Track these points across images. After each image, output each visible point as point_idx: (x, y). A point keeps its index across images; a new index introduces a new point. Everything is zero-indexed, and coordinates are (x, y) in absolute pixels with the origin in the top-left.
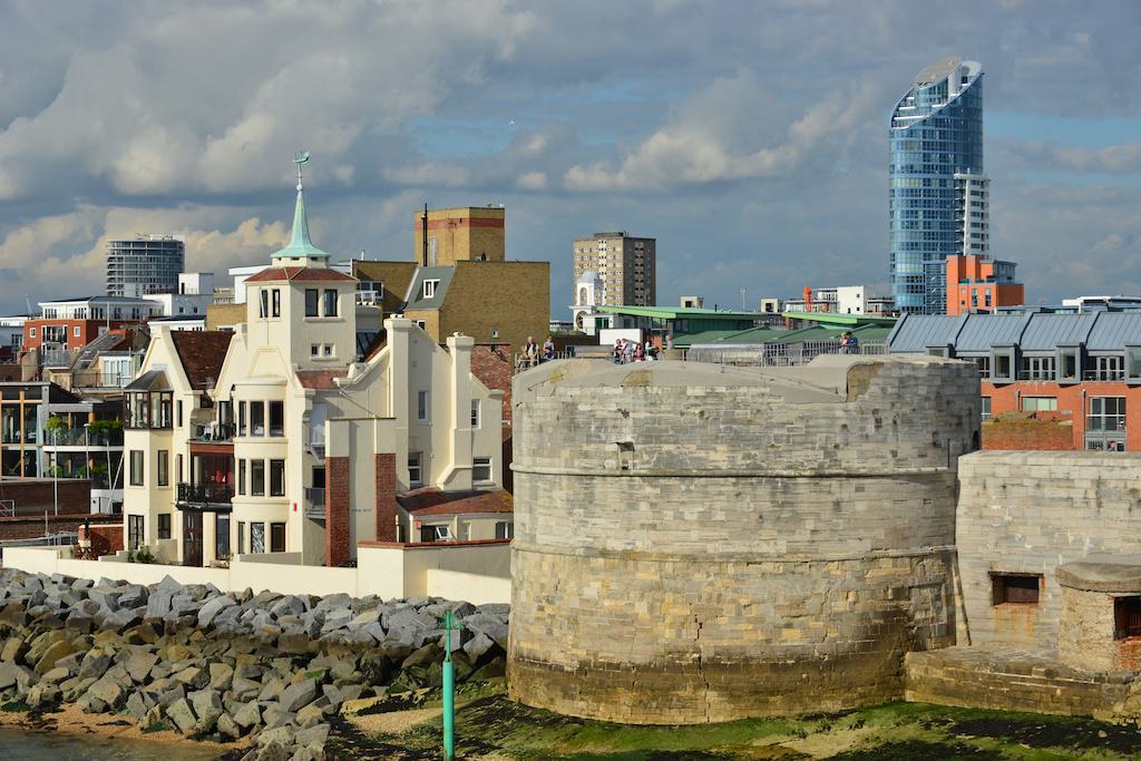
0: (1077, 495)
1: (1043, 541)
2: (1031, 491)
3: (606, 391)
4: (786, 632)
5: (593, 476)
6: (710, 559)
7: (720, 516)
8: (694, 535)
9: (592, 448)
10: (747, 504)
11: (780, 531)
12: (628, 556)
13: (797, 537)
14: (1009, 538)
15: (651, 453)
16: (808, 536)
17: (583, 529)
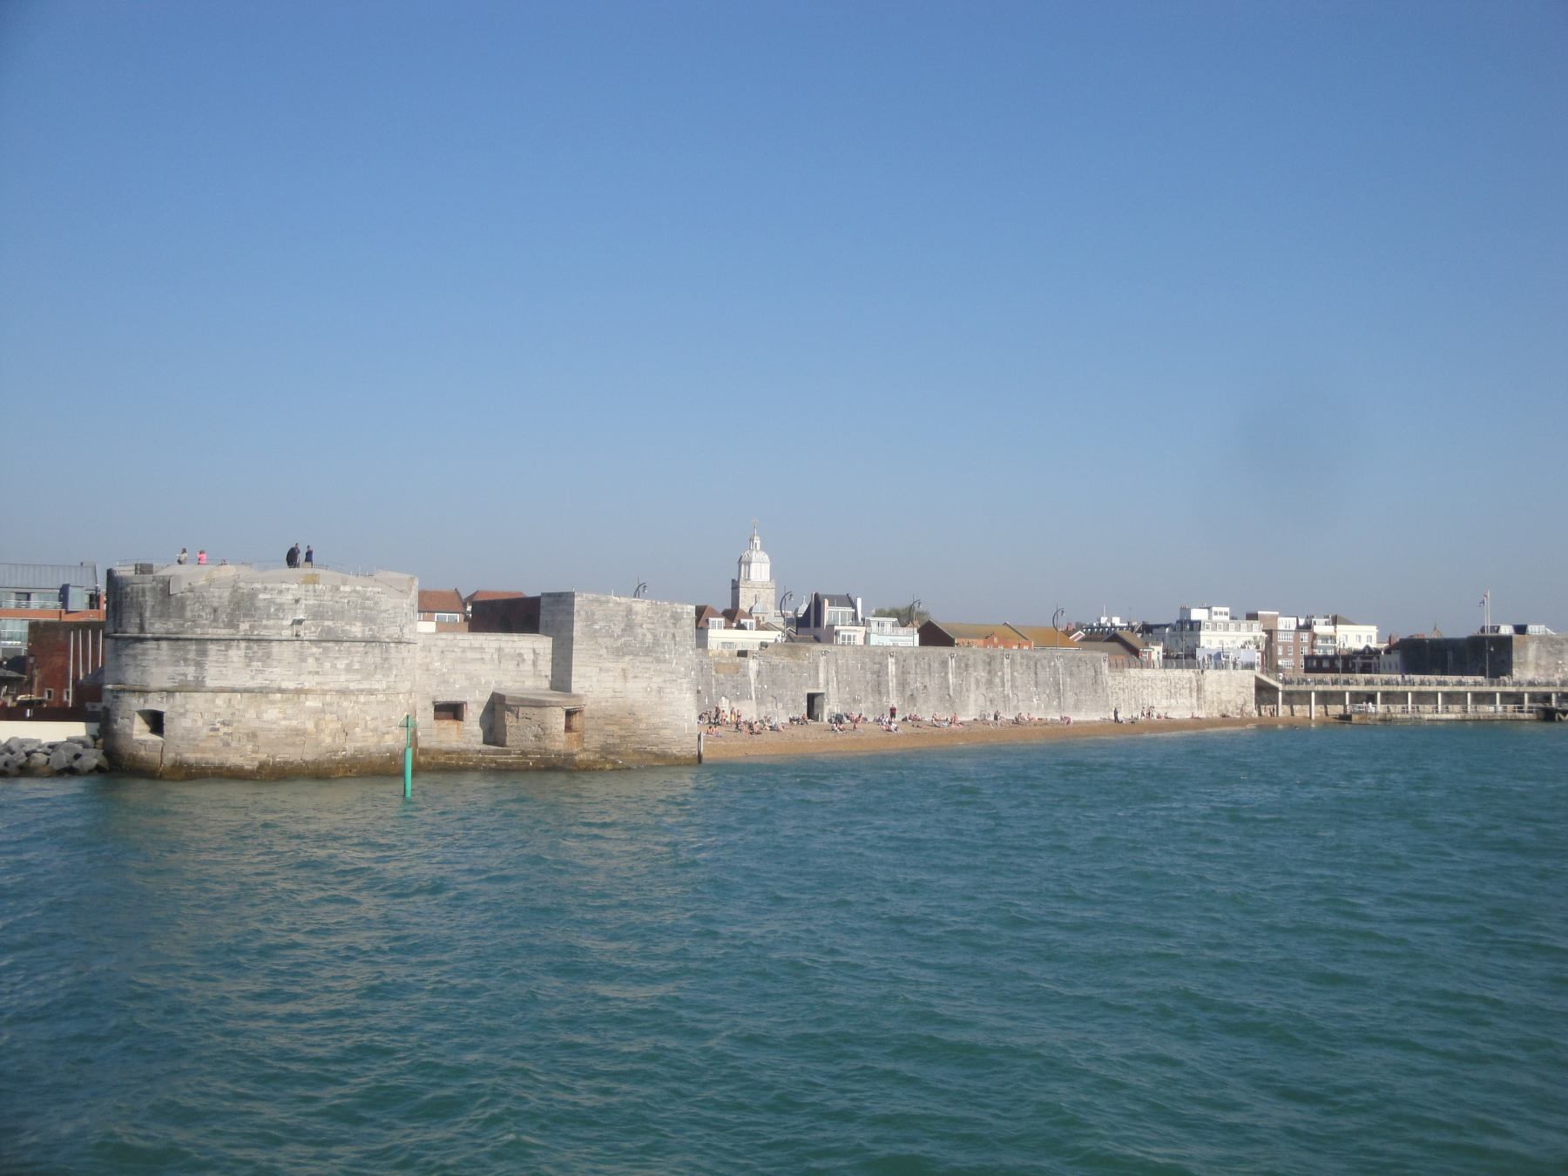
1: (466, 683)
6: (352, 692)
7: (357, 666)
8: (343, 678)
9: (271, 622)
10: (370, 659)
12: (299, 692)
14: (445, 682)
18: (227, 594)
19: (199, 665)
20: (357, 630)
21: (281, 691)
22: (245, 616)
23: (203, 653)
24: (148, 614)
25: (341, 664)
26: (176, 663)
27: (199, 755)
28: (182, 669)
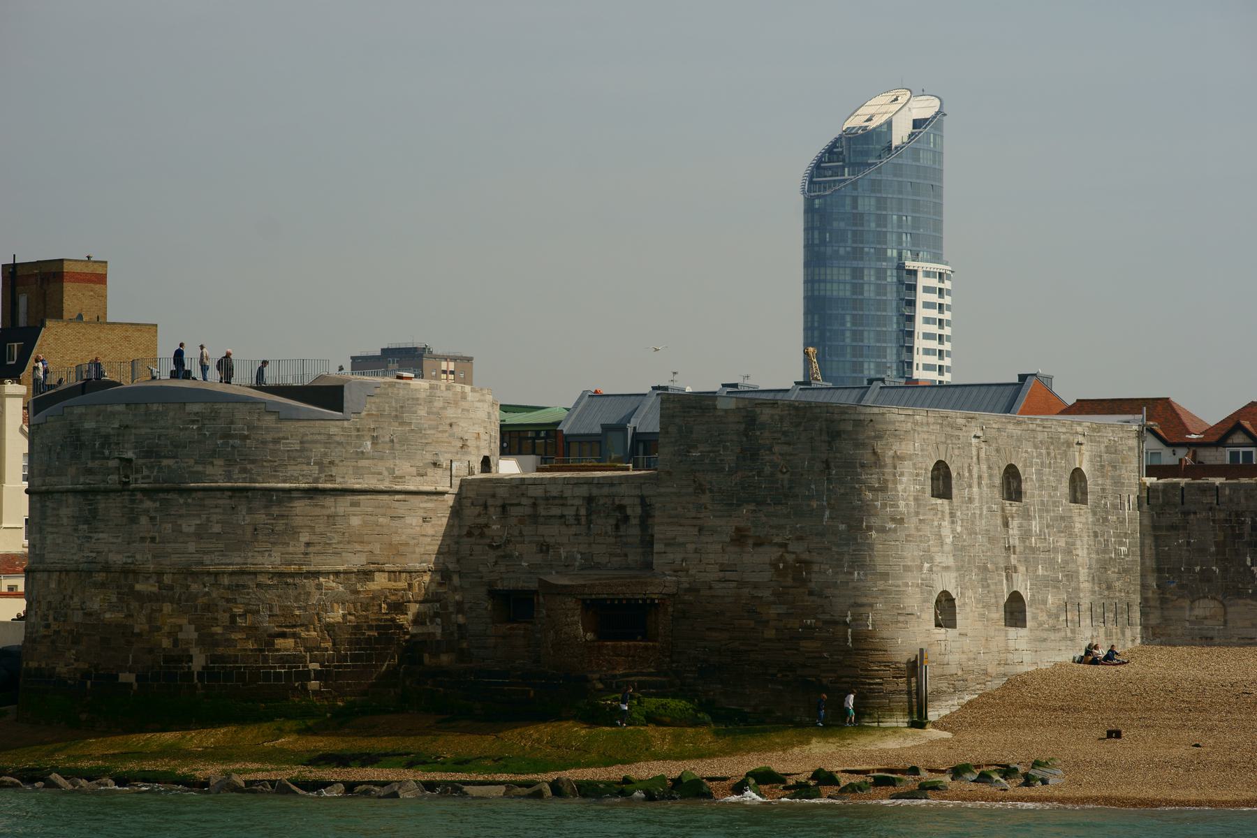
0: (569, 512)
1: (538, 558)
2: (528, 511)
4: (279, 642)
5: (95, 492)
7: (217, 528)
11: (274, 544)
13: (291, 549)
15: (151, 468)
16: (302, 549)
17: (87, 545)
20: (217, 476)
25: (189, 526)
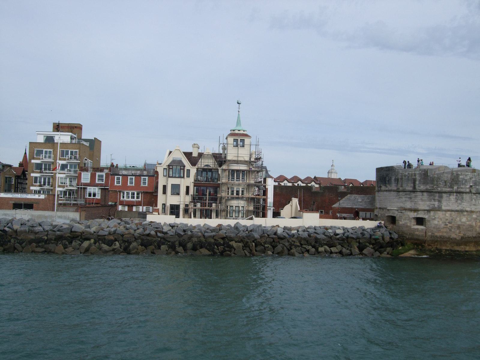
3: (467, 173)
9: (463, 186)
12: (472, 212)
18: (449, 176)
19: (440, 201)
21: (467, 211)
22: (456, 184)
23: (441, 197)
24: (417, 183)
26: (430, 200)
27: (441, 234)
28: (433, 202)
